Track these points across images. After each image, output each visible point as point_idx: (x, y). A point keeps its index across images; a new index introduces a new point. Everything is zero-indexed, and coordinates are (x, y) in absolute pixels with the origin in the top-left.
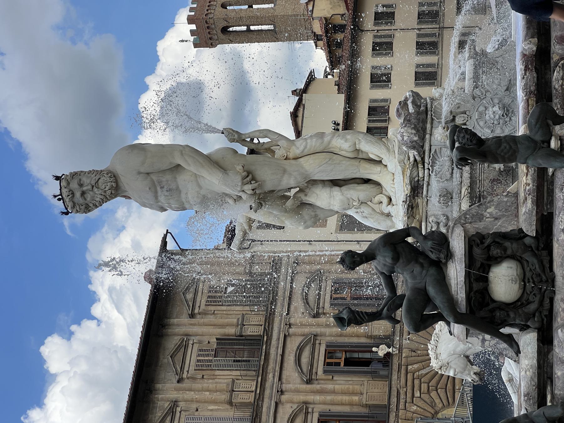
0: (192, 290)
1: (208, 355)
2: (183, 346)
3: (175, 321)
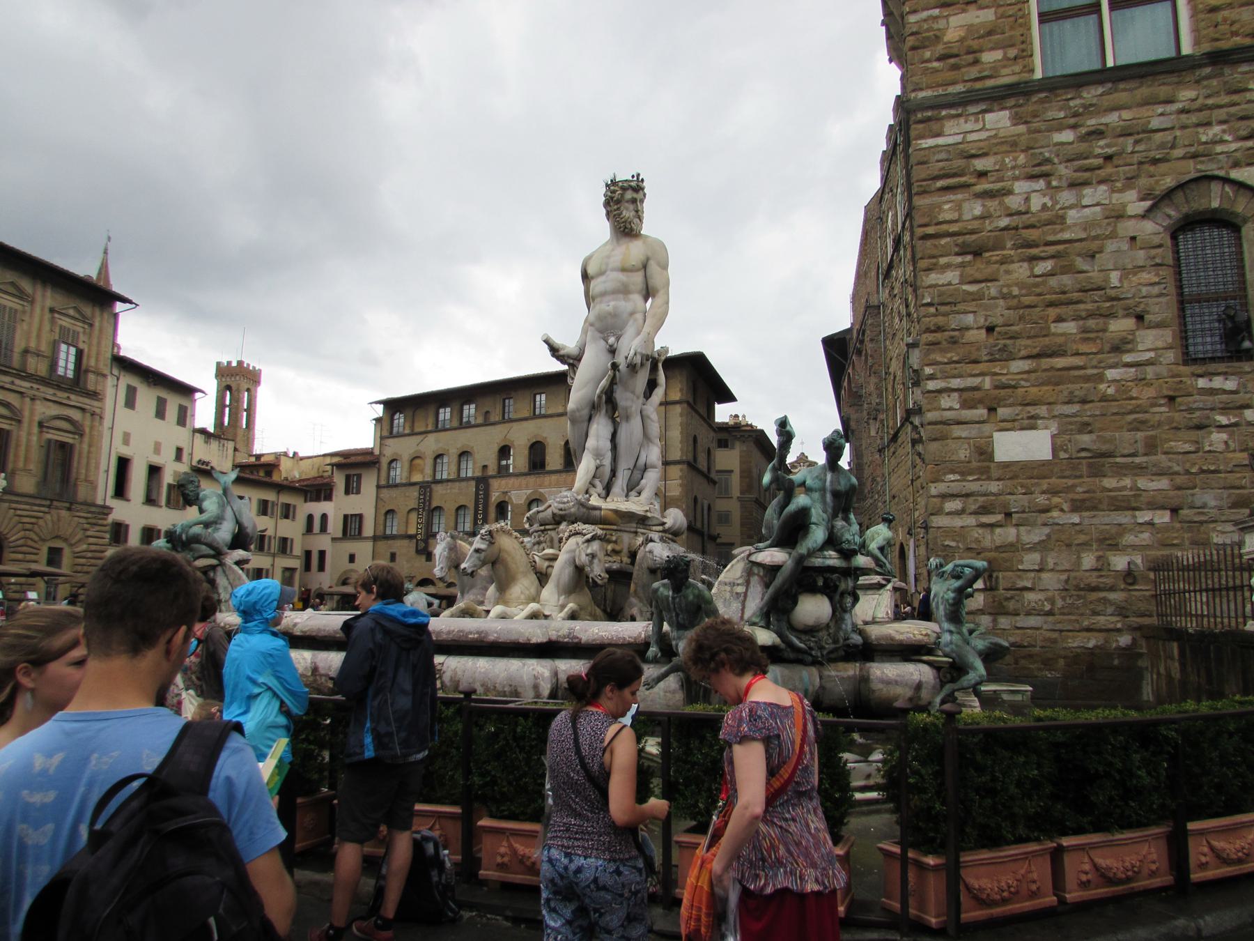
0: (77, 316)
1: (9, 317)
2: (21, 295)
3: (49, 293)
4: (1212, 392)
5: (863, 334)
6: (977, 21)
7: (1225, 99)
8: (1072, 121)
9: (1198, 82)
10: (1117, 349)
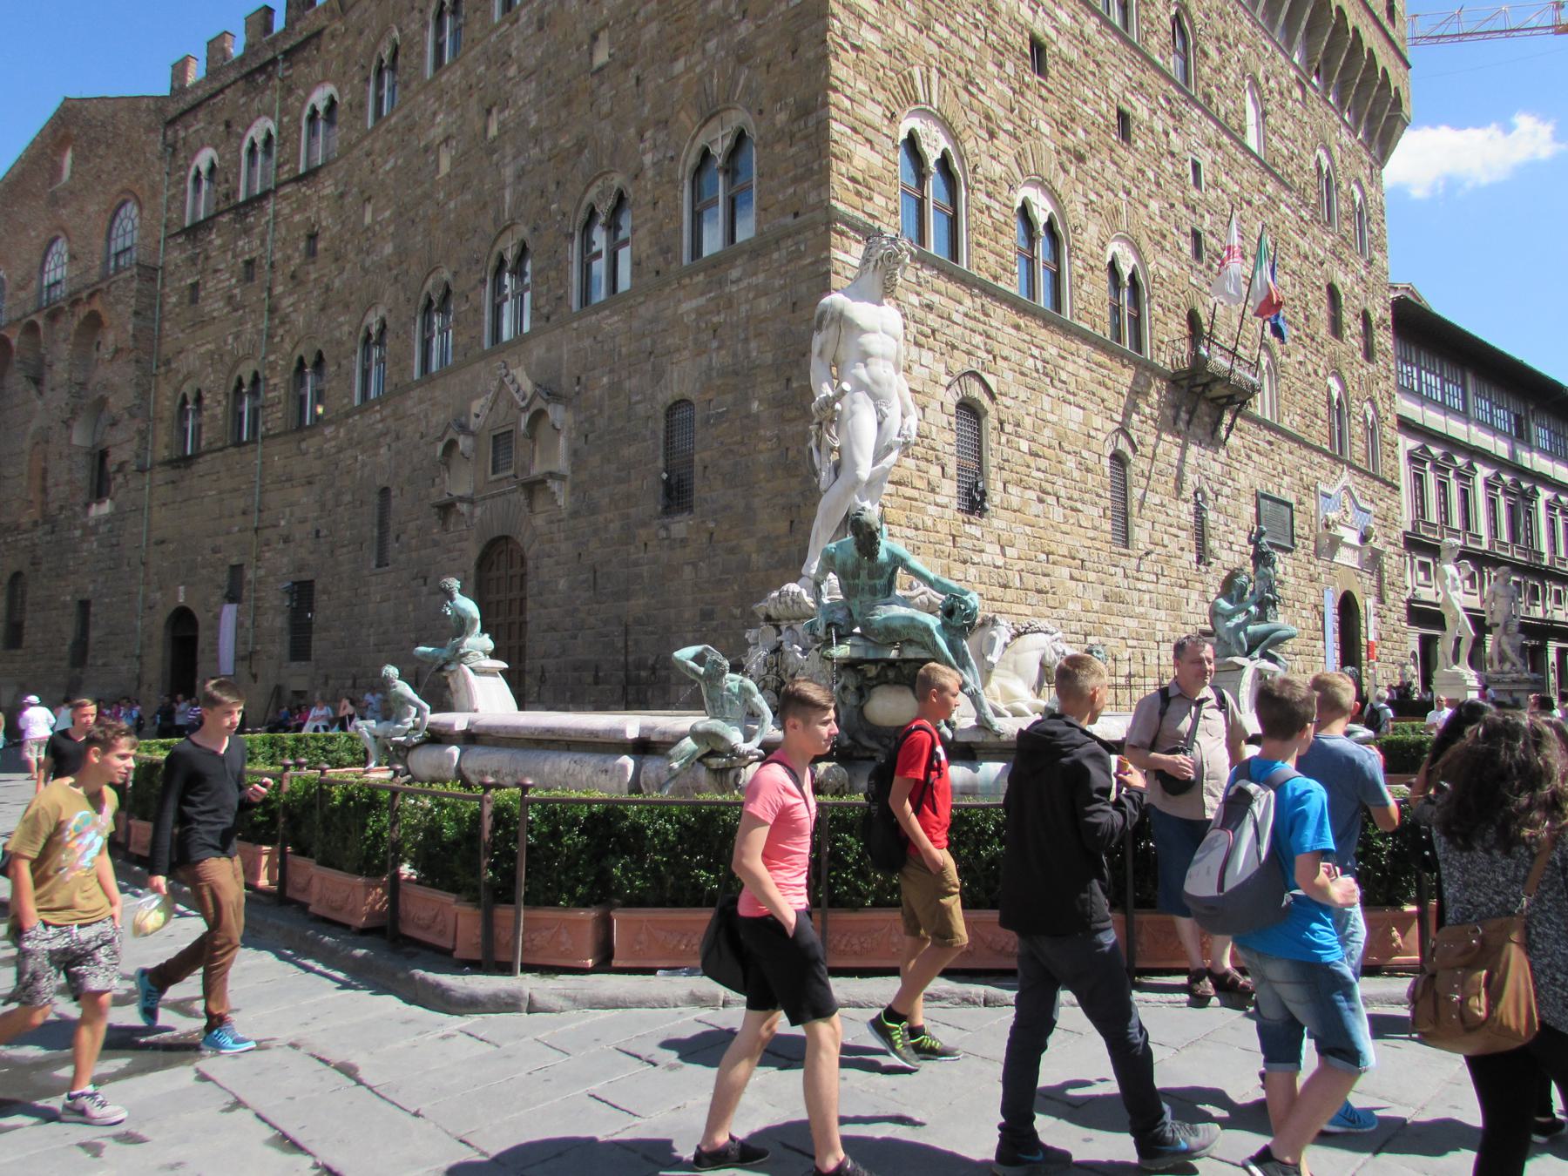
4: (972, 537)
5: (92, 296)
6: (872, 161)
7: (982, 318)
8: (918, 289)
9: (971, 295)
10: (933, 491)
